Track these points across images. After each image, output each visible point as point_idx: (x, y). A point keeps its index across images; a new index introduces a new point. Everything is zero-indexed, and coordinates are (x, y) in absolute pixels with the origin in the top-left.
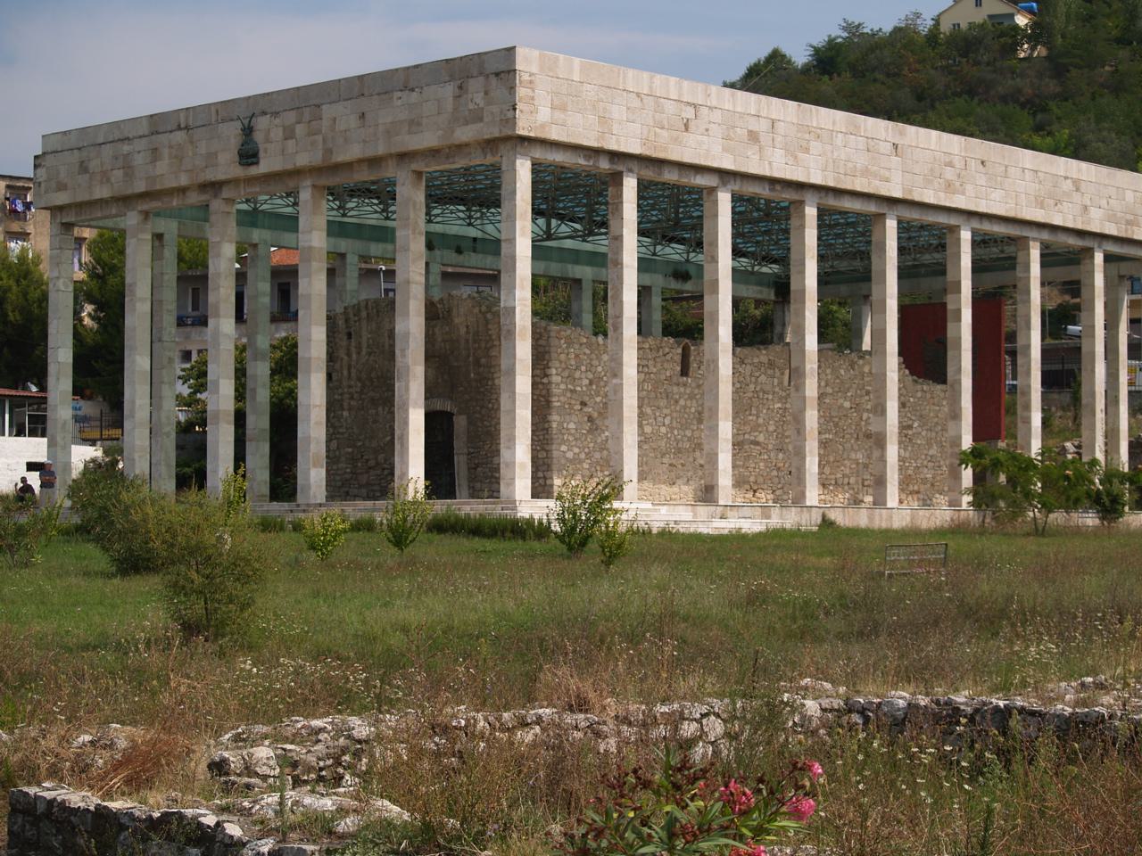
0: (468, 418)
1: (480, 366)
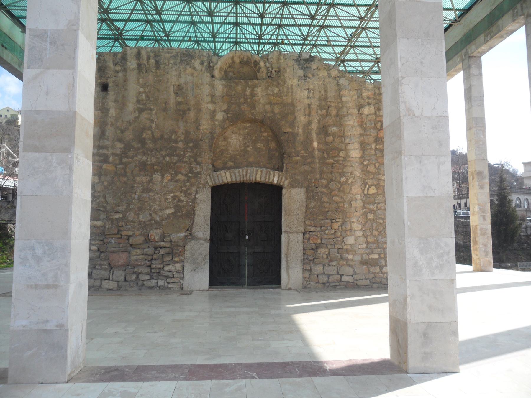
0: (307, 192)
1: (327, 134)
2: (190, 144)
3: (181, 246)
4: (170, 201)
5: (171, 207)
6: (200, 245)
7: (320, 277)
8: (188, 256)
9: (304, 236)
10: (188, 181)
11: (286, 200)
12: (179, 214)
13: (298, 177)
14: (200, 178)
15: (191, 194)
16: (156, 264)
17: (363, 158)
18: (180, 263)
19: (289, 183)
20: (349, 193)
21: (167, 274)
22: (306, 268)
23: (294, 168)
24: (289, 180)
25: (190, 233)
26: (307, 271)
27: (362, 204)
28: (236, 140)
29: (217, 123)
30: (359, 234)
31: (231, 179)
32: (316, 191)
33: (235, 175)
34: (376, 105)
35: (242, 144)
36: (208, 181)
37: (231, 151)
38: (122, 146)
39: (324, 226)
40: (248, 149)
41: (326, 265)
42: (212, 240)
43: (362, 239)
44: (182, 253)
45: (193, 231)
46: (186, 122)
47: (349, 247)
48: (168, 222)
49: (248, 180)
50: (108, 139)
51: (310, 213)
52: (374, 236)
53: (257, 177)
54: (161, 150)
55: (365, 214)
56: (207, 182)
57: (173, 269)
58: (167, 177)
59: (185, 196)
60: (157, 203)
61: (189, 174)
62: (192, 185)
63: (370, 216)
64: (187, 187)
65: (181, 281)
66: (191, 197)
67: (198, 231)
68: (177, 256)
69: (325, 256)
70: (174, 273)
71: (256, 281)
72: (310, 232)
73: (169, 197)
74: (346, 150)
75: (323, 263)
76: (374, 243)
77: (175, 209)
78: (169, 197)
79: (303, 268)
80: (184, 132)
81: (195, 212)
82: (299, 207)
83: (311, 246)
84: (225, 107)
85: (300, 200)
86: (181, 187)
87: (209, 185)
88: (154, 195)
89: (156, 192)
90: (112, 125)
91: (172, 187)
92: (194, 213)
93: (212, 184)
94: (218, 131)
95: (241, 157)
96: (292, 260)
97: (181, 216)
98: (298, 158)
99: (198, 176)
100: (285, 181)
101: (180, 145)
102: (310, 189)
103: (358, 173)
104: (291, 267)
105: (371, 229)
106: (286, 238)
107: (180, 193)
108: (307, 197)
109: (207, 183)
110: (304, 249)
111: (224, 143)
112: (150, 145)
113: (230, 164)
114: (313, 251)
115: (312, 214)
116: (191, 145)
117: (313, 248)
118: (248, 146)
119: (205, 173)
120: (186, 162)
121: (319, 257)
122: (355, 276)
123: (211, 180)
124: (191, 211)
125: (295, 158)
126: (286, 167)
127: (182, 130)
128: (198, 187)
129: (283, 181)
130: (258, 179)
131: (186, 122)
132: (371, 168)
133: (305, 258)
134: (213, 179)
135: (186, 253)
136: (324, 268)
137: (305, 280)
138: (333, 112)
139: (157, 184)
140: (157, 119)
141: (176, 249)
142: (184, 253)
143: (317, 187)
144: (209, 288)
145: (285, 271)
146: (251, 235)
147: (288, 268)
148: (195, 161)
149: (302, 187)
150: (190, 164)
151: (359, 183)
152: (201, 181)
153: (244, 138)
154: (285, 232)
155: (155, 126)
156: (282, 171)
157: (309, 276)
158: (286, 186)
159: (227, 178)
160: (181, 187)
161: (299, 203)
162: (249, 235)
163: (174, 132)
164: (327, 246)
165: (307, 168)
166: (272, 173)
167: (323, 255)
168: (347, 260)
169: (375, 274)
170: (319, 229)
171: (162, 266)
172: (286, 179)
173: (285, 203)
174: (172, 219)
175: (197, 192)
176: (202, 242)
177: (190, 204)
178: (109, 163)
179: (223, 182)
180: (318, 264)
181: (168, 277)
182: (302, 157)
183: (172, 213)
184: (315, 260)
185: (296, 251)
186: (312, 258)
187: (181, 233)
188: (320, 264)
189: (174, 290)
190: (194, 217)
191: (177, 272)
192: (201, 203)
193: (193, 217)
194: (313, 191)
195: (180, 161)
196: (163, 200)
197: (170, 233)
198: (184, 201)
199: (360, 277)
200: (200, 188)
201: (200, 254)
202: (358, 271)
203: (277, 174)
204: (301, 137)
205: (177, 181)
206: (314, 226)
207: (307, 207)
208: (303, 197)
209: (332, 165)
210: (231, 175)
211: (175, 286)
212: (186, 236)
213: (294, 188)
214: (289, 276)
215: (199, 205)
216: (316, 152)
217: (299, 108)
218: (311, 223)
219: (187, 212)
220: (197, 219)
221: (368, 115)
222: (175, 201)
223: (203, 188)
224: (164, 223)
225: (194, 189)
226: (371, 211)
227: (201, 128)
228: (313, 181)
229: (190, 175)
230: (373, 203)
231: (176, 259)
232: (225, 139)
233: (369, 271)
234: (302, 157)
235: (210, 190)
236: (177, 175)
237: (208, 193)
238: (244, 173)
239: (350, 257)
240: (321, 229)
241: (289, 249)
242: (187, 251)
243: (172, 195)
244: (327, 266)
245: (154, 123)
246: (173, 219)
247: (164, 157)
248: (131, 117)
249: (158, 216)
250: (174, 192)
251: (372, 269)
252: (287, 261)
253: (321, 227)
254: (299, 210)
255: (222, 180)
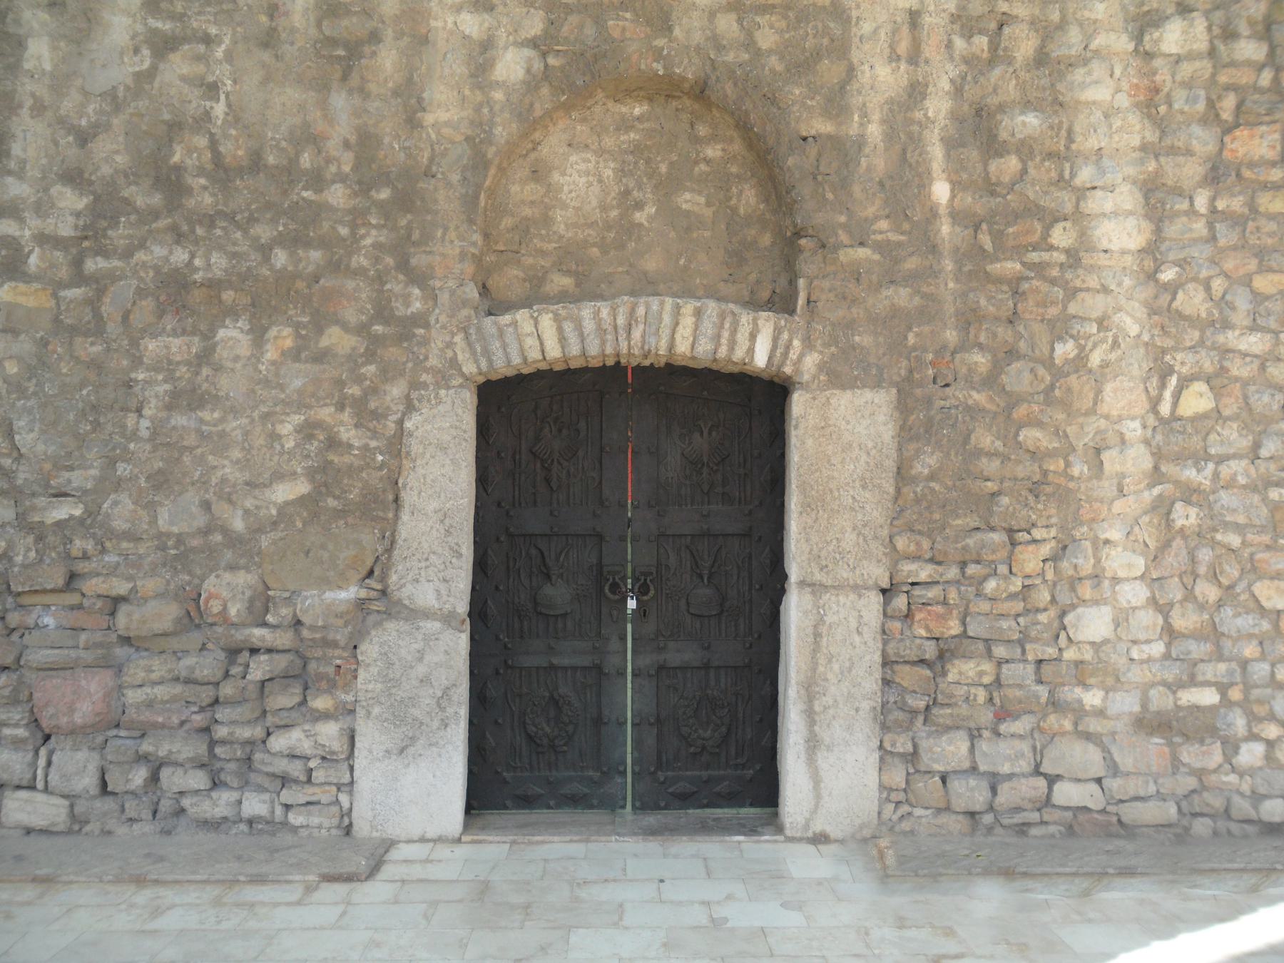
0: (903, 406)
1: (993, 147)
2: (378, 191)
3: (342, 643)
4: (290, 444)
5: (295, 473)
6: (427, 639)
7: (956, 785)
8: (370, 687)
9: (886, 603)
10: (370, 356)
11: (810, 442)
12: (332, 502)
13: (863, 339)
14: (425, 342)
15: (385, 417)
16: (233, 722)
17: (1153, 252)
18: (336, 719)
19: (821, 367)
20: (1092, 411)
21: (282, 765)
22: (893, 745)
23: (845, 298)
24: (821, 352)
25: (379, 587)
26: (896, 760)
27: (1148, 463)
28: (584, 180)
29: (498, 95)
30: (1134, 594)
31: (563, 347)
32: (942, 403)
33: (579, 328)
34: (1218, 16)
35: (613, 194)
36: (460, 357)
37: (562, 226)
38: (82, 203)
39: (978, 562)
40: (640, 217)
41: (986, 734)
42: (479, 613)
43: (1148, 620)
44: (344, 676)
45: (394, 578)
46: (363, 92)
47: (1088, 655)
48: (281, 539)
49: (636, 351)
50: (20, 175)
51: (918, 501)
52: (1202, 607)
53: (678, 337)
54: (252, 220)
55: (1163, 508)
56: (454, 363)
57: (306, 747)
58: (276, 338)
59: (356, 426)
60: (236, 454)
61: (376, 327)
62: (387, 373)
63: (1186, 516)
64: (368, 383)
65: (344, 799)
66: (385, 426)
67: (417, 581)
68: (325, 692)
69: (981, 695)
70: (312, 764)
71: (670, 790)
72: (913, 584)
73: (286, 429)
74: (1078, 217)
75: (972, 725)
76: (1197, 636)
77: (312, 479)
78: (286, 429)
79: (881, 747)
80: (353, 139)
81: (403, 494)
82: (868, 475)
83: (919, 647)
84: (535, 25)
85: (870, 444)
86: (340, 384)
87: (463, 375)
88: (222, 420)
89: (228, 403)
90: (39, 109)
91: (298, 383)
92: (396, 500)
93: (474, 370)
94: (502, 132)
95: (604, 252)
96: (831, 712)
97: (340, 514)
98: (863, 253)
99: (414, 335)
100: (801, 356)
101: (337, 196)
102: (918, 392)
103: (1131, 323)
104: (827, 740)
105: (1190, 574)
106: (806, 613)
107: (333, 409)
108: (902, 428)
109: (451, 367)
110: (886, 663)
111: (531, 191)
112: (203, 198)
113: (562, 282)
114: (928, 673)
115: (924, 504)
116: (384, 194)
117: (927, 657)
118: (639, 206)
119: (443, 318)
120: (360, 272)
121: (952, 696)
122: (1113, 784)
123: (474, 353)
124: (384, 491)
125: (850, 250)
126: (809, 295)
127: (343, 128)
128: (415, 385)
129: (793, 355)
130: (683, 347)
131: (363, 92)
132: (1192, 301)
133: (892, 700)
134: (479, 349)
135: (362, 675)
136: (973, 746)
137: (888, 800)
138: (1024, 45)
139: (232, 370)
140: (235, 82)
141: (317, 659)
142: (356, 677)
143: (947, 385)
144: (467, 826)
145: (803, 756)
146: (652, 592)
147: (813, 744)
148: (404, 265)
149: (877, 385)
150: (380, 279)
151: (1137, 364)
152: (426, 358)
153: (622, 170)
154: (802, 584)
155: (227, 114)
156: (791, 311)
157: (907, 782)
158: (806, 377)
159: (542, 344)
160: (340, 384)
161: (864, 457)
162: (641, 591)
163: (308, 137)
164: (989, 651)
165: (902, 296)
166: (745, 318)
167: (973, 690)
168: (1079, 712)
169: (1200, 773)
170: (953, 573)
171: (258, 732)
172: (808, 344)
173: (802, 456)
174: (299, 525)
175: (410, 407)
176: (433, 626)
177: (380, 458)
178: (27, 278)
179: (525, 359)
180: (948, 729)
181: (284, 780)
182: (882, 247)
183: (301, 500)
184: (935, 711)
185: (850, 670)
186: (922, 704)
187: (340, 588)
188: (958, 728)
189: (310, 836)
190: (397, 517)
191: (323, 758)
192: (428, 455)
193: (390, 515)
194: (929, 401)
195: (336, 267)
196: (261, 441)
197: (292, 588)
198: (350, 446)
199: (1133, 786)
200: (425, 385)
201: (425, 681)
202: (1126, 761)
203: (767, 323)
204: (876, 160)
205: (321, 357)
206: (932, 560)
207: (902, 474)
208: (882, 428)
209: (1015, 286)
210: (560, 330)
211: (315, 821)
212: (361, 604)
213: (843, 387)
214: (816, 780)
215: (419, 462)
216: (945, 229)
217: (867, 27)
218: (918, 544)
219: (365, 496)
220: (408, 527)
221: (1178, 60)
222: (313, 447)
223: (438, 385)
224: (265, 542)
225: (396, 391)
226: (1190, 494)
227: (429, 119)
228: (930, 357)
229: (378, 328)
230: (1200, 458)
231: (321, 703)
232: (538, 174)
233: (1176, 763)
234: (879, 247)
235: (468, 400)
236: (320, 330)
237: (460, 411)
238: (621, 321)
239: (1092, 698)
240: (963, 573)
241: (822, 661)
242: (369, 665)
243: (298, 419)
244: (990, 739)
245: (223, 97)
246: (304, 525)
247: (265, 251)
248: (120, 74)
249: (240, 513)
250: (309, 407)
251: (1190, 755)
252: (810, 716)
253: (963, 565)
254: (864, 487)
255: (522, 351)
